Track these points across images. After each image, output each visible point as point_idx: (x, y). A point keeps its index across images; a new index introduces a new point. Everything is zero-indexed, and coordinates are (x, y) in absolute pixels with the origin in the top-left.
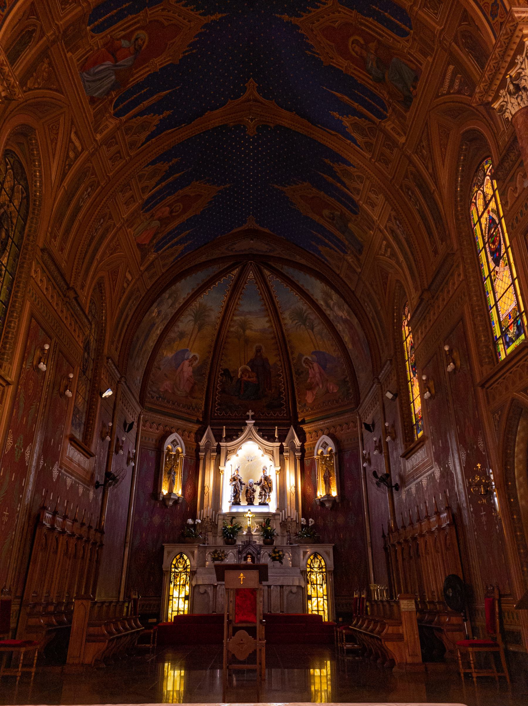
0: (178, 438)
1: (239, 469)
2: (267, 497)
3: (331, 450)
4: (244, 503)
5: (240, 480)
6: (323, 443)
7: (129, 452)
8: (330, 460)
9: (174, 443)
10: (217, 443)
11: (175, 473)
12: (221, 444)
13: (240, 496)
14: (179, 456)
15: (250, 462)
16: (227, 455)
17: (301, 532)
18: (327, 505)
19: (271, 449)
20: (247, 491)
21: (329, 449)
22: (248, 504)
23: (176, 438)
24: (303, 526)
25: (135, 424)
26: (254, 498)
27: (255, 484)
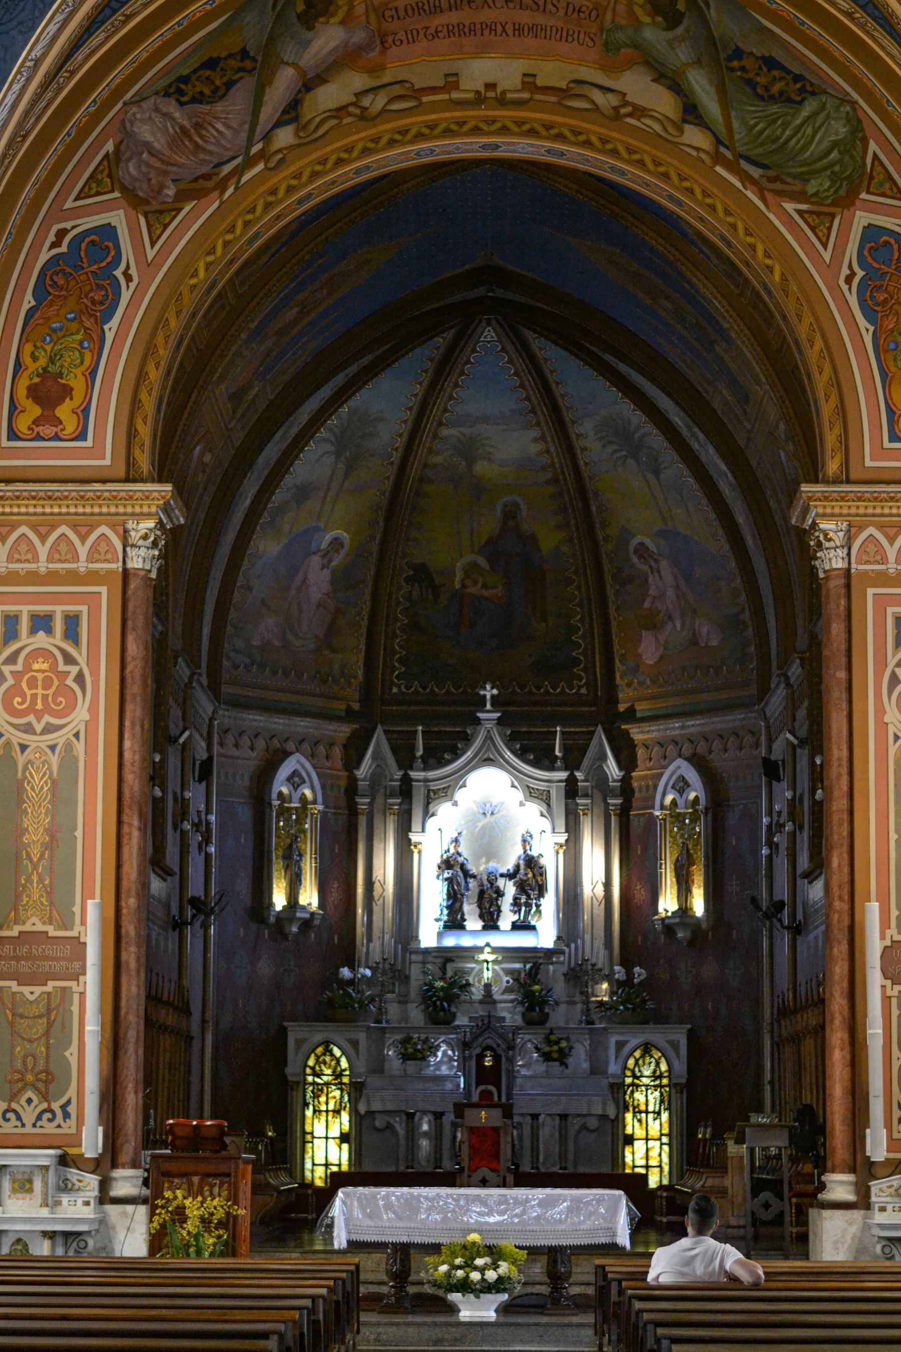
0: (303, 767)
1: (461, 839)
2: (534, 909)
4: (473, 923)
5: (462, 866)
9: (295, 780)
10: (401, 773)
11: (300, 855)
12: (413, 774)
15: (489, 819)
16: (428, 803)
19: (542, 786)
20: (481, 894)
22: (485, 928)
23: (299, 767)
26: (499, 911)
27: (502, 875)
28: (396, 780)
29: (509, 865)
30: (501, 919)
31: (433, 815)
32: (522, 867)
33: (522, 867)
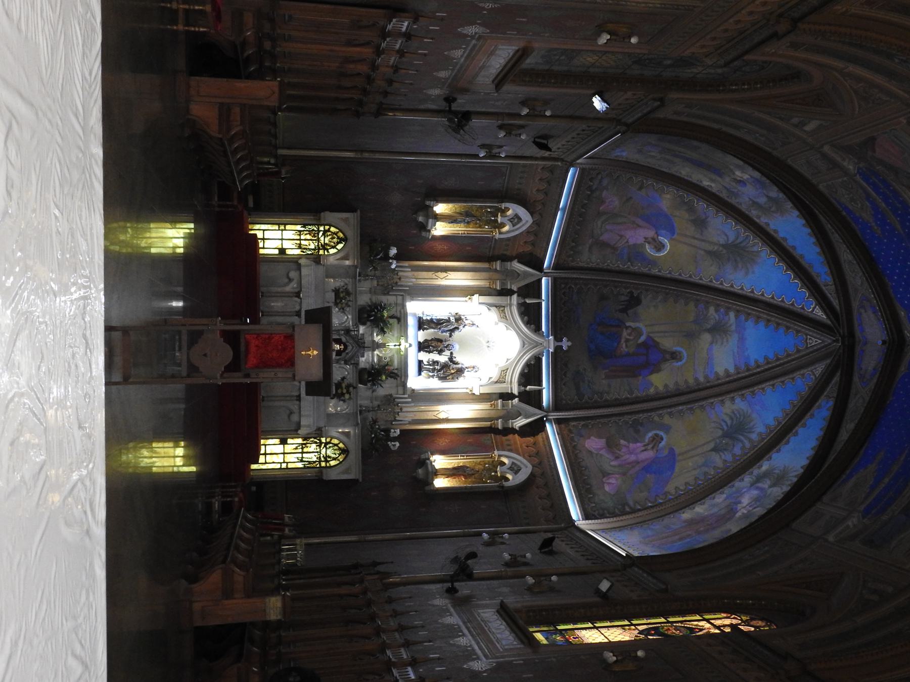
0: (523, 225)
1: (474, 327)
2: (431, 374)
3: (507, 479)
4: (422, 336)
5: (457, 328)
6: (519, 466)
7: (500, 147)
8: (491, 478)
9: (516, 219)
10: (515, 289)
11: (468, 223)
12: (515, 297)
13: (432, 330)
14: (495, 228)
15: (486, 344)
16: (496, 307)
17: (378, 429)
18: (420, 471)
19: (508, 378)
20: (440, 341)
21: (510, 477)
22: (419, 343)
23: (524, 222)
24: (387, 431)
25: (547, 154)
26: (430, 352)
27: (451, 353)
28: (511, 286)
29: (458, 358)
30: (425, 353)
31: (489, 309)
32: (457, 366)
33: (457, 366)
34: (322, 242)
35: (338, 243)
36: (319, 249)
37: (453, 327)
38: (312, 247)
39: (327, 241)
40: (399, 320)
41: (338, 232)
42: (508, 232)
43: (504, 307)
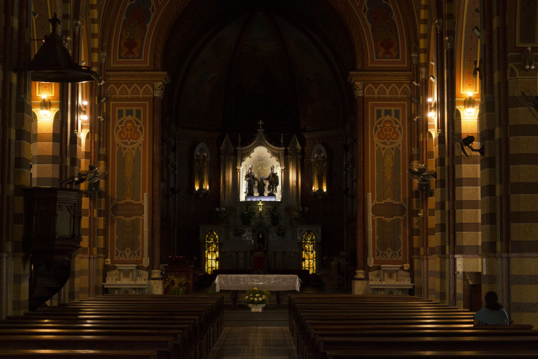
2: (275, 189)
4: (256, 194)
16: (242, 157)
19: (277, 152)
26: (264, 190)
27: (265, 179)
29: (267, 176)
31: (244, 161)
32: (271, 177)
33: (271, 177)
34: (213, 241)
35: (213, 234)
36: (216, 243)
37: (252, 179)
38: (215, 246)
39: (212, 239)
40: (248, 205)
41: (208, 234)
42: (207, 153)
43: (242, 154)
